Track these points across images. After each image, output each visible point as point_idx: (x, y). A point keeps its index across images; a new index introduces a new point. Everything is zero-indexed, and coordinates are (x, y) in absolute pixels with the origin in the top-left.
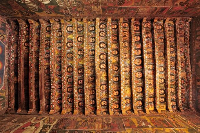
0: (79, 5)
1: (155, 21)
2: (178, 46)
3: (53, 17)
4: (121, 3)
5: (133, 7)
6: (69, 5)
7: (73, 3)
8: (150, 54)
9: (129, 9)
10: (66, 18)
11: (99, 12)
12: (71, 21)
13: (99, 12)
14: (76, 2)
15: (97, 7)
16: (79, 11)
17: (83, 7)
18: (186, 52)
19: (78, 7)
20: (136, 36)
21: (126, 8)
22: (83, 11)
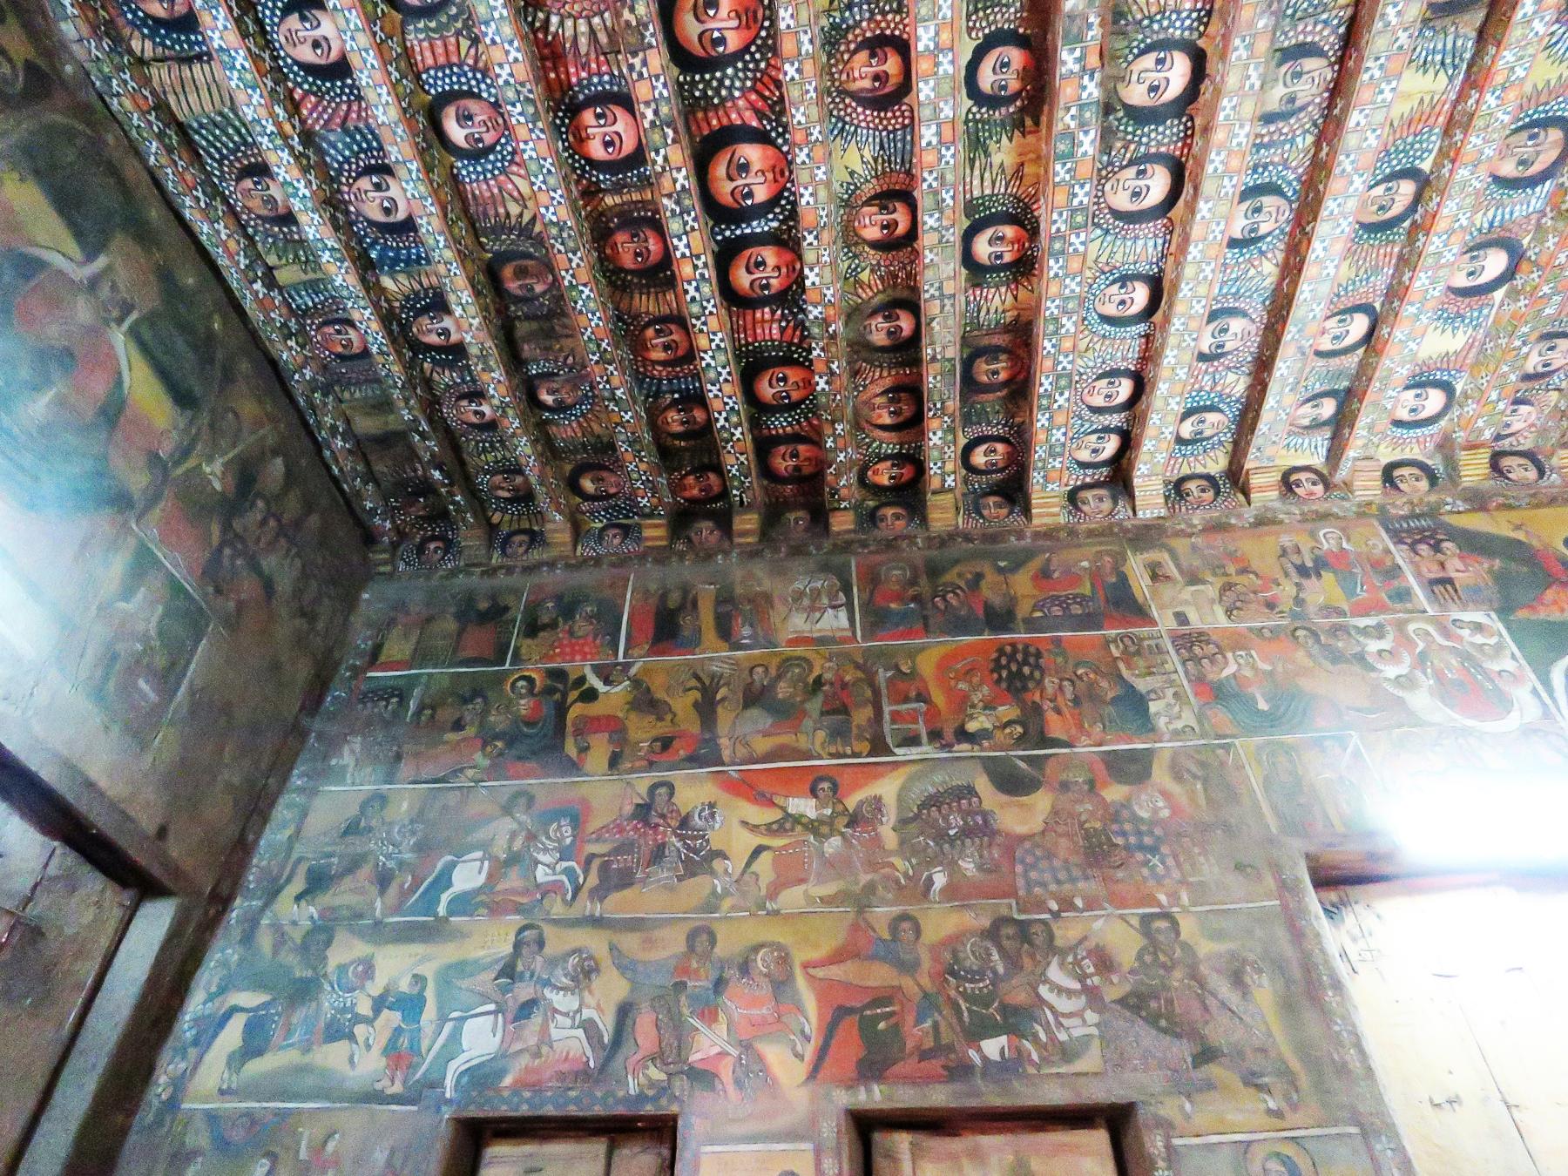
0: (1335, 630)
1: (657, 526)
2: (396, 368)
3: (1552, 501)
4: (1014, 668)
5: (908, 634)
6: (1411, 627)
7: (1385, 644)
8: (632, 272)
9: (925, 618)
10: (1433, 498)
11: (1154, 577)
12: (1385, 461)
13: (1156, 574)
14: (1361, 658)
15: (1182, 618)
16: (1327, 576)
17: (1295, 616)
18: (284, 325)
19: (1344, 615)
20: (797, 405)
21: (960, 625)
22: (1287, 575)
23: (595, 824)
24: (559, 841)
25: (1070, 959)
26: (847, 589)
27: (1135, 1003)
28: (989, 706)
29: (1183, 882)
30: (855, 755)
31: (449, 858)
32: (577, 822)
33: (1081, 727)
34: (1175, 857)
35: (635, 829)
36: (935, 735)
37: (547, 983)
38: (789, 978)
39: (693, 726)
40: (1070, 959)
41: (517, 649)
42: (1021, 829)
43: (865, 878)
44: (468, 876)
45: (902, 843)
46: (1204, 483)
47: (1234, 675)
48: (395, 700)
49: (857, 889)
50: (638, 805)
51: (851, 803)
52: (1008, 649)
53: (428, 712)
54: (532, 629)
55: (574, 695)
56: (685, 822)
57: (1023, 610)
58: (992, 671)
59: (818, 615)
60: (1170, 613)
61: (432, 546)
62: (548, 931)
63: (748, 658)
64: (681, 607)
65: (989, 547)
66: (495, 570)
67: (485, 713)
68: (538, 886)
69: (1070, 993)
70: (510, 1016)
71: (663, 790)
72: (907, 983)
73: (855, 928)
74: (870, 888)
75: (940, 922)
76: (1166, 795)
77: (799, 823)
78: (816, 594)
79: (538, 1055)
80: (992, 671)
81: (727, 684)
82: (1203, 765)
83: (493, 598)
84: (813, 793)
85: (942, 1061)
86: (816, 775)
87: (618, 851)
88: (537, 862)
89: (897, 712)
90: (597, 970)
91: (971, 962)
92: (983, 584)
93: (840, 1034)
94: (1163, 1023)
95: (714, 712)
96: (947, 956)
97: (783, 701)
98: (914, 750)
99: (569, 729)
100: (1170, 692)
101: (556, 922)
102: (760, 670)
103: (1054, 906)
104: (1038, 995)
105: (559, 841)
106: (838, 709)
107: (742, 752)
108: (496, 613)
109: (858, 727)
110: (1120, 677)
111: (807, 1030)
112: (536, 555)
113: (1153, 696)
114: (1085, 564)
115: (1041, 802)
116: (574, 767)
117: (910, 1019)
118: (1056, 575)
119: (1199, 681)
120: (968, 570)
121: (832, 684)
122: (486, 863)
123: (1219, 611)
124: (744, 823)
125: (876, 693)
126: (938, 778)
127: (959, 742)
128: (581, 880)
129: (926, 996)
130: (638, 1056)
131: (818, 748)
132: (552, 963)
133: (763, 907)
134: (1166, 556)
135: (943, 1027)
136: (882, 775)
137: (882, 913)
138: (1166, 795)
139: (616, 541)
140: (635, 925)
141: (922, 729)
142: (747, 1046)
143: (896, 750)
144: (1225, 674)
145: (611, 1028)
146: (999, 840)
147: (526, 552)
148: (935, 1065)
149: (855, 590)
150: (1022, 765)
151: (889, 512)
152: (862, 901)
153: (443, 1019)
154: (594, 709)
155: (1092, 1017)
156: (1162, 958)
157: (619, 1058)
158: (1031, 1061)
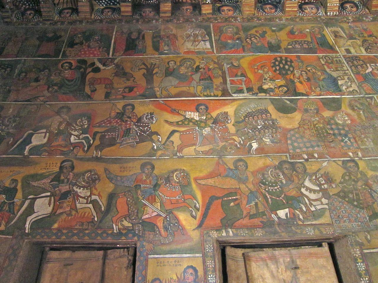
9: (243, 47)
11: (336, 36)
13: (336, 35)
15: (348, 51)
21: (259, 50)
23: (98, 120)
24: (81, 126)
25: (314, 178)
26: (209, 34)
27: (343, 195)
28: (272, 79)
29: (359, 148)
30: (215, 96)
31: (31, 131)
32: (90, 119)
33: (311, 89)
34: (354, 138)
35: (117, 122)
36: (249, 90)
37: (75, 184)
38: (189, 184)
39: (143, 83)
40: (314, 178)
41: (64, 52)
42: (289, 127)
43: (221, 144)
44: (38, 140)
45: (237, 131)
46: (352, 5)
47: (371, 72)
48: (8, 69)
49: (218, 148)
50: (118, 113)
51: (214, 114)
52: (279, 59)
53: (24, 74)
54: (72, 44)
55: (90, 70)
56: (139, 120)
57: (284, 45)
58: (272, 67)
59: (197, 43)
60: (343, 49)
61: (29, 12)
62: (75, 162)
63: (168, 58)
64: (138, 38)
65: (268, 23)
66: (56, 23)
67: (49, 76)
68: (71, 144)
69: (315, 191)
70: (57, 198)
71: (129, 107)
72: (243, 187)
73: (218, 164)
74: (224, 148)
75: (256, 163)
76: (348, 115)
77: (192, 122)
78: (196, 36)
79: (69, 214)
80: (272, 67)
81: (158, 67)
82: (362, 104)
83: (55, 32)
84: (197, 110)
85: (261, 219)
86: (199, 103)
87: (107, 131)
88: (71, 134)
89: (233, 80)
90: (99, 179)
91: (271, 178)
92: (266, 35)
93: (213, 207)
94: (355, 203)
95: (152, 78)
96: (260, 176)
97: (182, 74)
98: (241, 95)
99: (87, 82)
100: (346, 77)
101: (81, 159)
102: (172, 62)
103: (306, 157)
104: (302, 193)
105: (81, 126)
106: (207, 78)
107: (165, 93)
108: (56, 38)
109: (216, 85)
110: (326, 71)
111: (197, 205)
112: (74, 17)
113: (339, 78)
114: (308, 30)
115: (297, 116)
116: (89, 97)
117: (244, 202)
118: (296, 33)
119: (357, 74)
120: (260, 30)
121: (204, 69)
122: (48, 134)
123: (363, 50)
124: (167, 121)
125: (224, 73)
126: (252, 106)
127: (260, 93)
128: (92, 142)
129: (251, 192)
130: (118, 216)
131: (199, 93)
132: (77, 176)
133: (176, 155)
134: (340, 29)
135: (260, 205)
136: (227, 104)
137: (230, 158)
138: (348, 115)
139: (109, 14)
140: (116, 161)
141: (244, 87)
142: (170, 212)
143: (233, 95)
144: (367, 72)
145: (105, 203)
146: (279, 130)
147: (70, 16)
148: (256, 221)
149: (213, 35)
150: (288, 102)
151: (225, 8)
152: (221, 153)
153: (25, 198)
154: (98, 75)
155: (324, 201)
156: (353, 177)
157: (109, 216)
158: (300, 219)
